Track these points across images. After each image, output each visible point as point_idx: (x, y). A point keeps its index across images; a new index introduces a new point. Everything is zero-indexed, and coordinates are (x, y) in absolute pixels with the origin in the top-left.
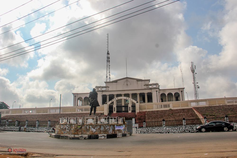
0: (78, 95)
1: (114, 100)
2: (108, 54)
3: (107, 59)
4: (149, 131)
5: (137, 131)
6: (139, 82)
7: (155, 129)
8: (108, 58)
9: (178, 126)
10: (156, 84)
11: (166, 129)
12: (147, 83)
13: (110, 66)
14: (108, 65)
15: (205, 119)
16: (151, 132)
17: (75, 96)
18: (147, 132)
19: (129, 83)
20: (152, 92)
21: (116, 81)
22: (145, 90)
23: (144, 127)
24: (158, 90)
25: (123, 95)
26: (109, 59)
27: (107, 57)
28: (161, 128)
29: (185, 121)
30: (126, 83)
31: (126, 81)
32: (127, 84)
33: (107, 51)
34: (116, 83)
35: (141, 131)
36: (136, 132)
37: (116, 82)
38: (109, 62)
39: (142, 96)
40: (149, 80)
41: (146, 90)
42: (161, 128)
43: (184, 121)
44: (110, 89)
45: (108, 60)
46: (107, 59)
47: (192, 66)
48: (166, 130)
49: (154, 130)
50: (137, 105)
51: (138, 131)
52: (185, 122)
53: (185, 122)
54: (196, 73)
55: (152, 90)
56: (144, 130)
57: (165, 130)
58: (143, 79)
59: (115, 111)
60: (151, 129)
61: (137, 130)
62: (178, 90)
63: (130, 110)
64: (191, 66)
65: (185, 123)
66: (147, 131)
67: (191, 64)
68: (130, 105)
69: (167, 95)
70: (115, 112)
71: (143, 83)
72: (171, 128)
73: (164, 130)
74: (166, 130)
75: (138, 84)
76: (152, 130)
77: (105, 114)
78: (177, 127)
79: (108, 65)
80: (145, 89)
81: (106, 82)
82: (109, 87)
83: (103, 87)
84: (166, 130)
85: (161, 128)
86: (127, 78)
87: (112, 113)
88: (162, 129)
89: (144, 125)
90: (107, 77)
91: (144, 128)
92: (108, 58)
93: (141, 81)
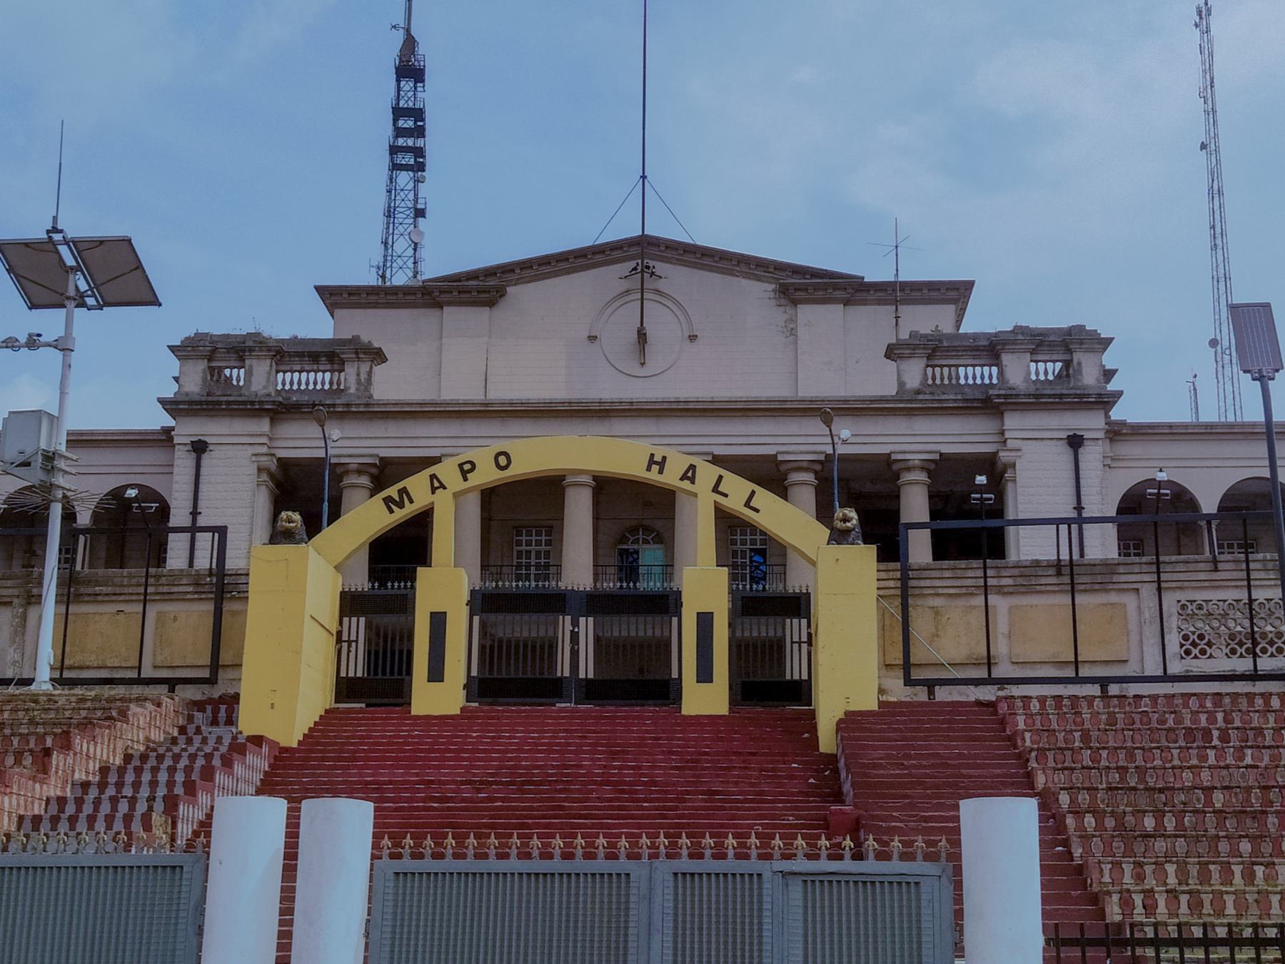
1: (436, 485)
2: (409, 70)
3: (399, 133)
6: (806, 312)
8: (408, 121)
12: (926, 320)
13: (420, 213)
14: (404, 204)
19: (661, 323)
20: (1004, 456)
22: (910, 412)
24: (1090, 423)
26: (420, 132)
27: (398, 113)
30: (627, 318)
31: (625, 285)
32: (642, 336)
33: (400, 36)
37: (491, 304)
38: (421, 167)
41: (923, 426)
44: (390, 384)
50: (842, 585)
55: (1014, 422)
59: (436, 673)
63: (705, 674)
68: (704, 585)
70: (438, 696)
75: (793, 332)
79: (404, 204)
82: (378, 356)
83: (287, 354)
92: (408, 121)
93: (847, 303)
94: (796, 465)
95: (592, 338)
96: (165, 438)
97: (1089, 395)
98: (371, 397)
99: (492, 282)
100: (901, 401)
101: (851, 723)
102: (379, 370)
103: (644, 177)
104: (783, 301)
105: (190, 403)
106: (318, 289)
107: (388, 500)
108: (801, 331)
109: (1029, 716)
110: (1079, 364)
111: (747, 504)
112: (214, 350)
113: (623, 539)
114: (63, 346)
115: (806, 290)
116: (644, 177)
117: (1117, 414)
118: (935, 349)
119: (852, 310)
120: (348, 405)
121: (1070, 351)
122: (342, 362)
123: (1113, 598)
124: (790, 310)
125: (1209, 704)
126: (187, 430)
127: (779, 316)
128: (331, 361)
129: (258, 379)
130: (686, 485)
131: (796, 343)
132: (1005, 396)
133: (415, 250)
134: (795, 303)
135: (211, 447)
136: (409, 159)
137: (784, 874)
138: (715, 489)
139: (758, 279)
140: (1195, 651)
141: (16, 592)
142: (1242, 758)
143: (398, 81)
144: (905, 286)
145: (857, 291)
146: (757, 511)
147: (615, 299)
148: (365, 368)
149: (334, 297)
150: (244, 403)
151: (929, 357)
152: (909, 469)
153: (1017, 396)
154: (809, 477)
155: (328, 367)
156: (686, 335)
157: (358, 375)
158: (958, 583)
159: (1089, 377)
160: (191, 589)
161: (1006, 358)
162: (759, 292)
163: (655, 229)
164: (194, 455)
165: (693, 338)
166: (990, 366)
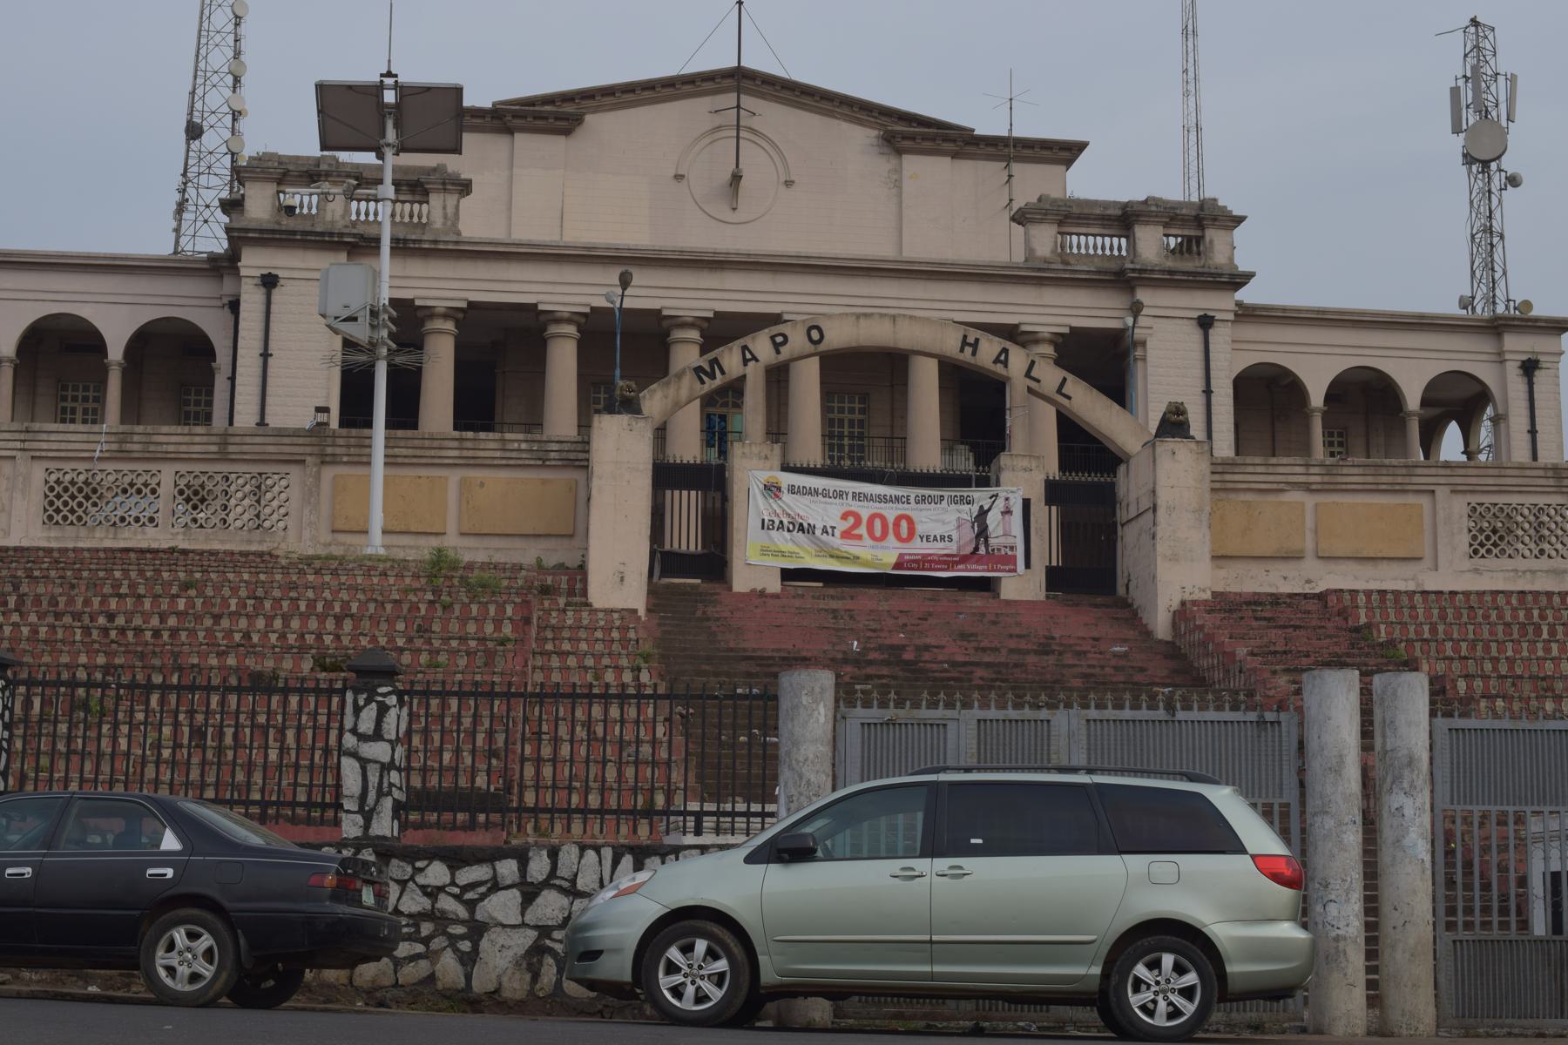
1: (748, 357)
6: (914, 165)
10: (1200, 222)
19: (755, 162)
24: (1219, 303)
25: (694, 334)
31: (718, 120)
34: (561, 139)
37: (567, 132)
40: (1066, 152)
41: (1051, 296)
47: (1474, 77)
54: (1513, 181)
58: (988, 125)
62: (1485, 344)
64: (1452, 66)
67: (1456, 45)
69: (1317, 399)
75: (898, 185)
80: (1035, 276)
86: (740, 80)
90: (194, 131)
93: (955, 156)
95: (679, 177)
97: (1221, 275)
98: (459, 234)
99: (569, 108)
101: (1182, 614)
102: (466, 202)
104: (886, 150)
105: (261, 231)
108: (907, 186)
110: (1211, 242)
111: (1059, 391)
112: (284, 174)
115: (913, 139)
117: (1247, 295)
118: (1071, 215)
120: (435, 242)
121: (1202, 227)
122: (426, 193)
123: (1411, 499)
124: (894, 161)
125: (1514, 601)
126: (254, 262)
127: (884, 165)
130: (999, 368)
131: (900, 195)
133: (237, 25)
134: (899, 152)
135: (282, 282)
138: (1028, 375)
140: (1483, 551)
141: (308, 450)
145: (967, 143)
146: (1069, 398)
147: (704, 135)
148: (451, 200)
150: (322, 234)
151: (1060, 223)
153: (1152, 271)
155: (409, 197)
156: (783, 179)
157: (444, 208)
158: (1271, 478)
159: (1219, 258)
160: (498, 454)
162: (861, 137)
163: (748, 63)
164: (263, 290)
166: (1119, 237)
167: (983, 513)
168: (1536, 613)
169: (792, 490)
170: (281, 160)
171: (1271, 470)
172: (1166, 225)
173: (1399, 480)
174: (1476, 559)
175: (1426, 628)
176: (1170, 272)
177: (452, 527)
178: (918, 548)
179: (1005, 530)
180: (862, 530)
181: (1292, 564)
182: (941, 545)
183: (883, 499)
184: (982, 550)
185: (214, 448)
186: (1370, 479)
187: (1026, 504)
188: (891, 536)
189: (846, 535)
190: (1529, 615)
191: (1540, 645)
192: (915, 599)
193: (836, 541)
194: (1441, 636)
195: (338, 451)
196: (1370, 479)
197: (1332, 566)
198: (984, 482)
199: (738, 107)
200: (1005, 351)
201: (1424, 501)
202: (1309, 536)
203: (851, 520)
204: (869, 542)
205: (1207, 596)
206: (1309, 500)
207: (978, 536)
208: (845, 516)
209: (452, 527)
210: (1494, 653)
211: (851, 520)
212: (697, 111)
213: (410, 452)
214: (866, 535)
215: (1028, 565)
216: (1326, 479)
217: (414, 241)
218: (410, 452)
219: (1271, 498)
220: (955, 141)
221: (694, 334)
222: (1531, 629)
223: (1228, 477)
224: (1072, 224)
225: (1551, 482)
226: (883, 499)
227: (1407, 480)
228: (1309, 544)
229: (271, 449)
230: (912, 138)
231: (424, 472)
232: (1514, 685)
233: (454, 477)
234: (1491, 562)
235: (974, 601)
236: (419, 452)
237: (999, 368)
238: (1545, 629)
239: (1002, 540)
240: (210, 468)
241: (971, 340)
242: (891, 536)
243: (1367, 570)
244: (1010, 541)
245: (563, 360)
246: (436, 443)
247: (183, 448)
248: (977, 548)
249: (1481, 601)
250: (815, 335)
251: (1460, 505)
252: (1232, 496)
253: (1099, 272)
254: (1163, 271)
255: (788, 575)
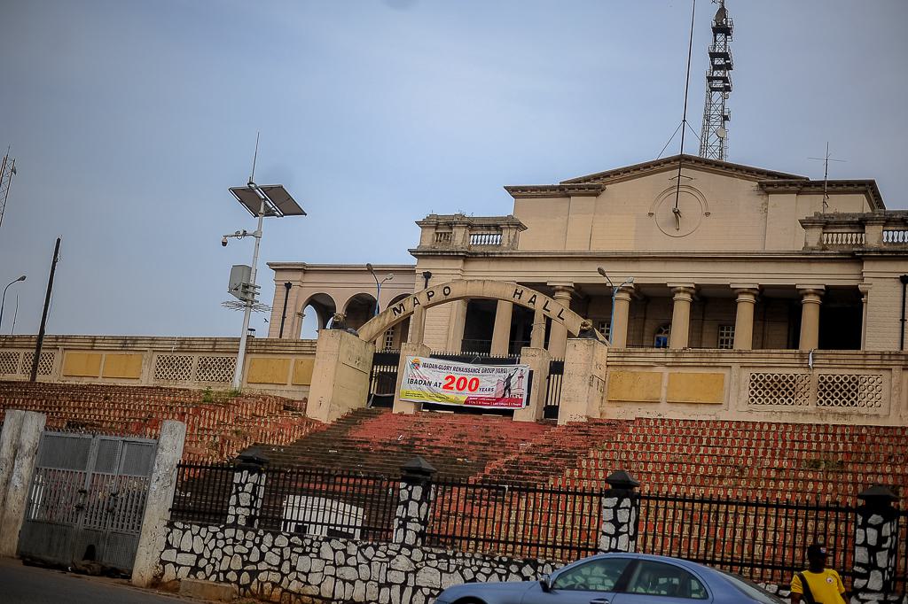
0: (311, 278)
2: (722, 29)
4: (262, 576)
5: (170, 555)
6: (774, 199)
7: (317, 565)
8: (721, 61)
9: (535, 565)
11: (416, 571)
13: (726, 118)
14: (715, 113)
15: (875, 519)
16: (274, 584)
17: (288, 286)
18: (245, 578)
19: (689, 205)
21: (590, 187)
22: (809, 261)
23: (230, 519)
26: (729, 67)
27: (713, 55)
28: (370, 562)
29: (623, 516)
32: (677, 213)
35: (201, 556)
36: (163, 563)
37: (597, 195)
38: (728, 89)
39: (777, 309)
40: (868, 188)
41: (816, 268)
42: (369, 552)
43: (616, 508)
44: (526, 243)
45: (720, 73)
46: (716, 67)
48: (408, 591)
49: (303, 563)
51: (179, 551)
52: (618, 525)
53: (618, 525)
56: (228, 550)
57: (403, 586)
58: (815, 176)
60: (287, 554)
61: (168, 546)
65: (617, 534)
66: (245, 563)
71: (811, 205)
72: (460, 569)
73: (389, 585)
74: (416, 588)
76: (286, 567)
77: (311, 413)
78: (528, 571)
81: (512, 190)
83: (472, 225)
84: (416, 588)
85: (370, 562)
86: (682, 161)
87: (383, 410)
88: (375, 566)
89: (238, 505)
91: (229, 533)
92: (721, 61)
93: (798, 193)
94: (741, 290)
96: (410, 271)
99: (597, 183)
100: (803, 254)
102: (522, 234)
103: (684, 121)
106: (505, 188)
107: (395, 309)
109: (650, 428)
111: (559, 316)
112: (438, 224)
113: (660, 331)
114: (257, 236)
116: (684, 121)
118: (827, 223)
119: (801, 197)
120: (501, 253)
122: (501, 230)
123: (720, 371)
124: (765, 198)
127: (759, 201)
128: (497, 230)
129: (459, 238)
132: (862, 252)
134: (768, 193)
136: (719, 84)
137: (124, 441)
138: (544, 308)
139: (748, 179)
142: (699, 451)
143: (715, 36)
144: (830, 184)
145: (804, 186)
148: (513, 232)
149: (516, 192)
150: (449, 252)
151: (824, 228)
152: (807, 294)
153: (870, 252)
154: (751, 298)
158: (647, 360)
161: (868, 229)
165: (707, 214)
167: (510, 377)
168: (723, 432)
169: (424, 365)
170: (438, 217)
171: (648, 355)
172: (884, 225)
173: (713, 360)
174: (752, 405)
175: (642, 437)
176: (881, 252)
177: (289, 383)
178: (478, 394)
179: (519, 387)
180: (454, 385)
181: (654, 406)
182: (488, 393)
183: (467, 370)
184: (507, 396)
185: (211, 347)
186: (698, 360)
187: (531, 373)
188: (467, 388)
189: (446, 387)
190: (719, 433)
191: (677, 447)
192: (468, 418)
193: (440, 390)
194: (633, 440)
195: (253, 347)
196: (698, 360)
197: (674, 407)
198: (513, 362)
199: (680, 175)
200: (535, 296)
201: (726, 372)
202: (664, 391)
203: (450, 380)
204: (455, 390)
205: (584, 420)
206: (666, 371)
207: (505, 389)
208: (447, 378)
209: (289, 383)
210: (629, 449)
211: (450, 380)
212: (665, 178)
213: (278, 348)
214: (455, 387)
215: (528, 404)
216: (675, 360)
217: (492, 254)
218: (278, 348)
219: (647, 370)
220: (795, 185)
221: (566, 295)
222: (697, 440)
223: (625, 359)
224: (832, 228)
225: (798, 361)
226: (467, 370)
227: (717, 360)
228: (663, 395)
229: (230, 347)
230: (772, 185)
231: (283, 357)
232: (610, 464)
233: (293, 358)
234: (759, 406)
235: (497, 421)
236: (282, 348)
237: (530, 306)
238: (705, 440)
239: (517, 391)
240: (208, 355)
241: (519, 292)
242: (467, 388)
243: (693, 409)
244: (521, 391)
245: (745, 313)
246: (287, 344)
247: (201, 347)
248: (504, 395)
249: (648, 424)
250: (447, 291)
251: (746, 375)
252: (629, 369)
253: (841, 254)
254: (876, 252)
255: (418, 406)
